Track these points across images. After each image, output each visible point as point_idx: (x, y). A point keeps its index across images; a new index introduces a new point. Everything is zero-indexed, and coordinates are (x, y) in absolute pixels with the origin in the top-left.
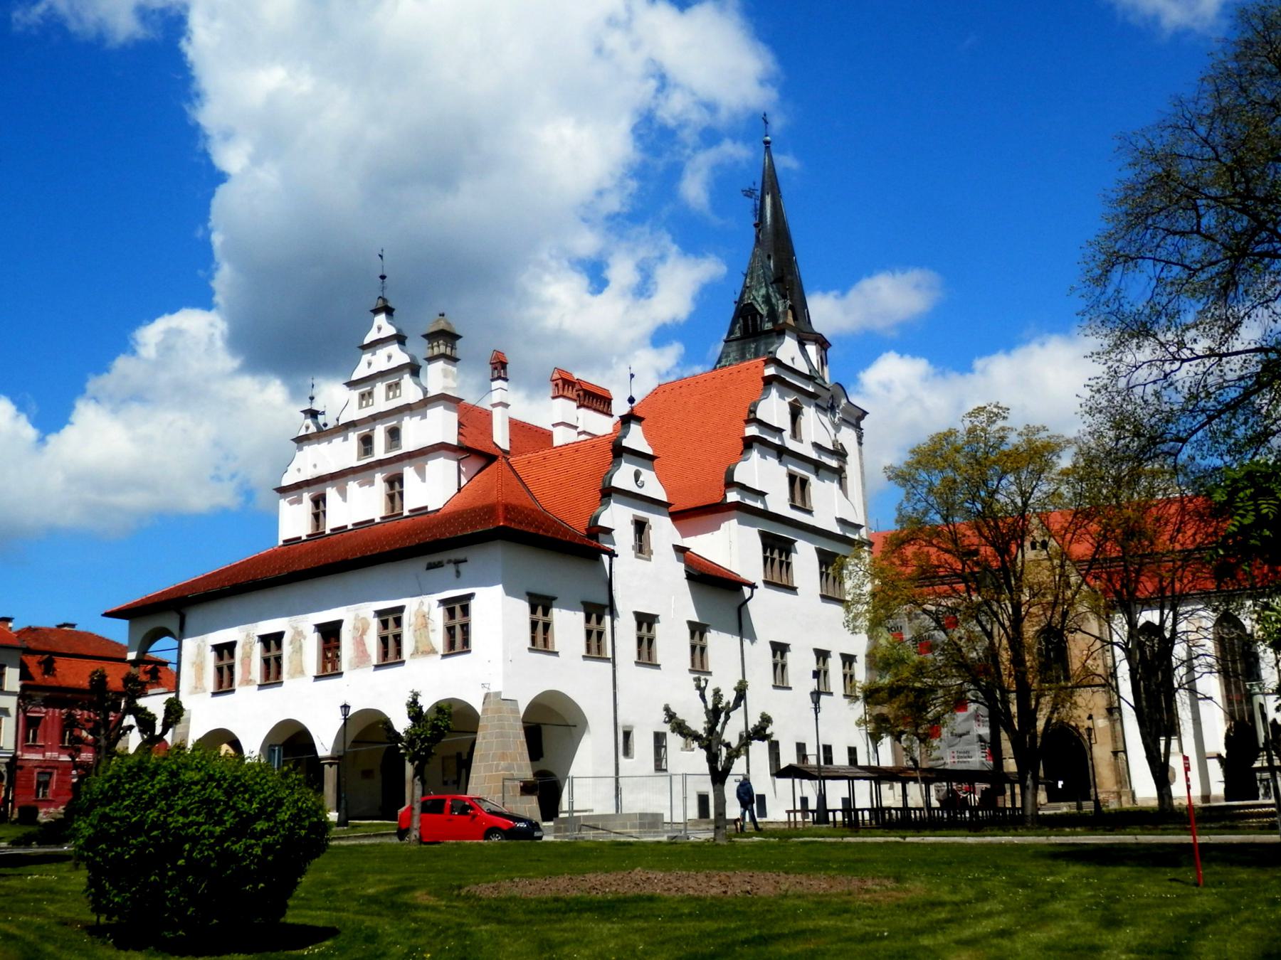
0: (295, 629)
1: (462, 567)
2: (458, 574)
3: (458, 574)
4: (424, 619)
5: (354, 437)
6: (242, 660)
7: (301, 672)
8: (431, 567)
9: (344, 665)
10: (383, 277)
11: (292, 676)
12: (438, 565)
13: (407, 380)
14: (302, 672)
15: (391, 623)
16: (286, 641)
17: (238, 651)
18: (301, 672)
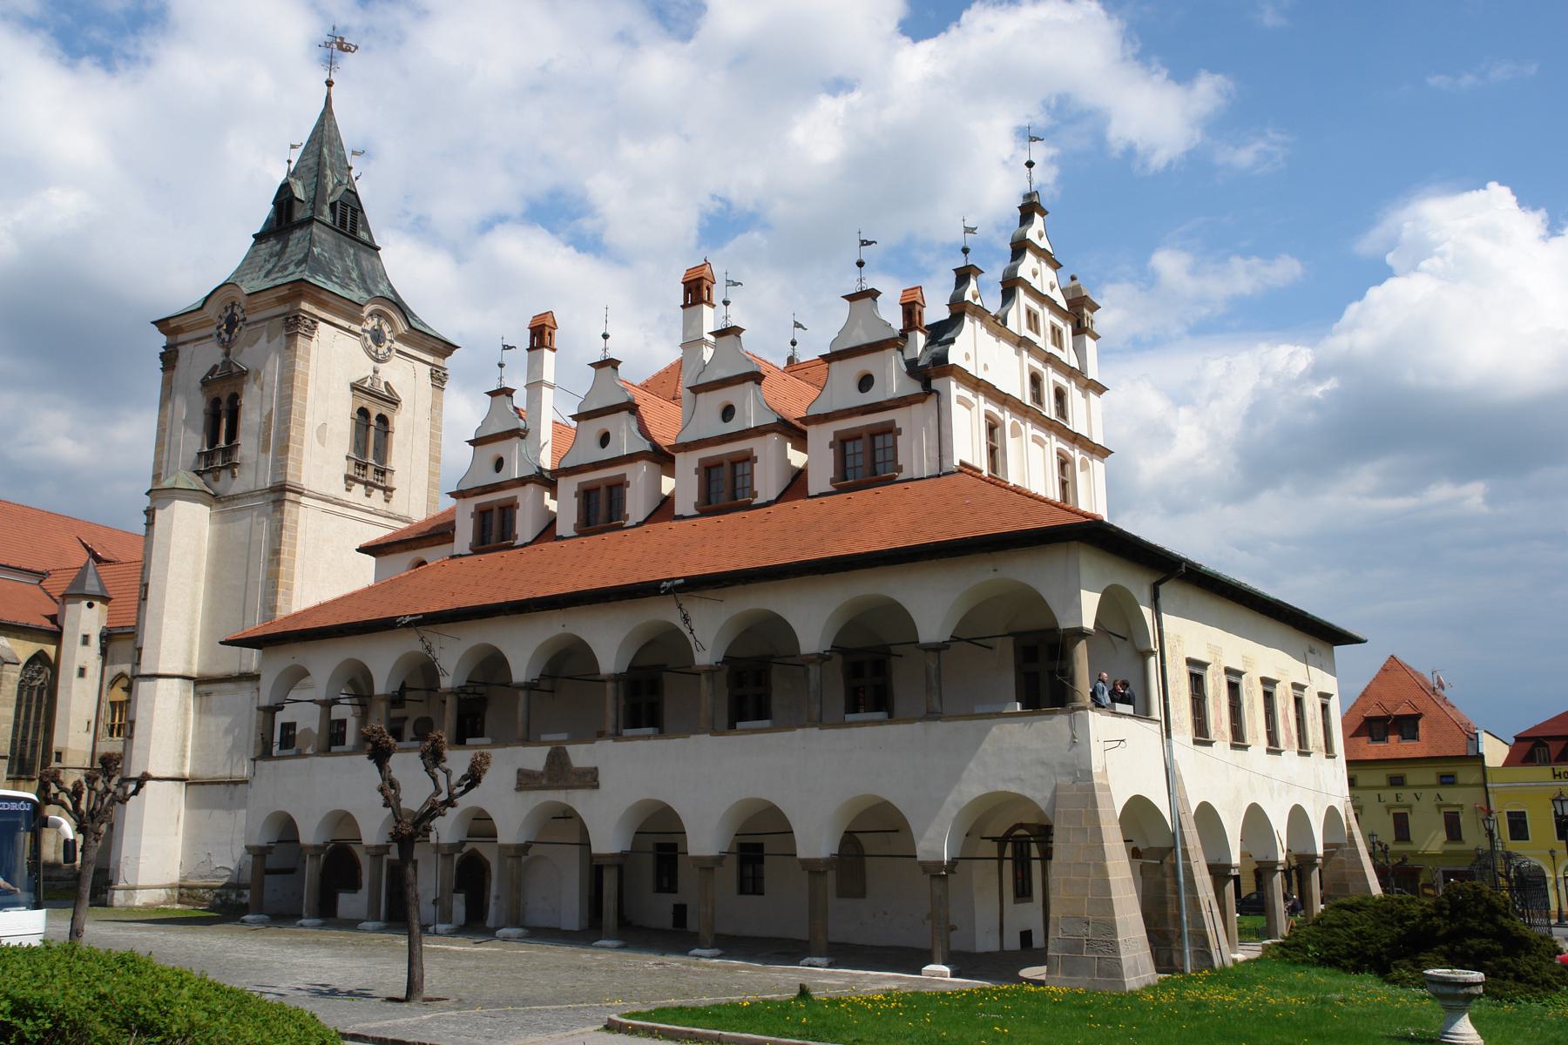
13: (1067, 331)
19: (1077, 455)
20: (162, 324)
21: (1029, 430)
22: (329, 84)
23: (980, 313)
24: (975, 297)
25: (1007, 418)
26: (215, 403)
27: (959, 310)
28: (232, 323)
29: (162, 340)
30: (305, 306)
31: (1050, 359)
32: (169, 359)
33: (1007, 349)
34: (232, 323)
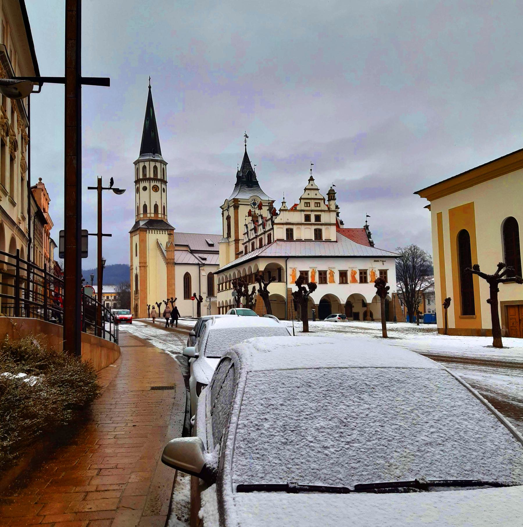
0: (331, 271)
1: (384, 263)
2: (383, 264)
3: (383, 264)
4: (374, 274)
5: (303, 214)
6: (311, 277)
7: (333, 281)
8: (375, 261)
9: (349, 282)
10: (311, 170)
11: (330, 282)
12: (378, 261)
14: (334, 282)
15: (363, 273)
16: (328, 273)
17: (310, 274)
18: (333, 281)
19: (323, 228)
20: (221, 207)
21: (303, 227)
22: (246, 145)
23: (283, 210)
24: (284, 207)
25: (294, 228)
26: (228, 223)
27: (280, 210)
28: (229, 207)
29: (222, 210)
30: (236, 203)
31: (312, 211)
32: (223, 214)
33: (299, 213)
34: (229, 207)
